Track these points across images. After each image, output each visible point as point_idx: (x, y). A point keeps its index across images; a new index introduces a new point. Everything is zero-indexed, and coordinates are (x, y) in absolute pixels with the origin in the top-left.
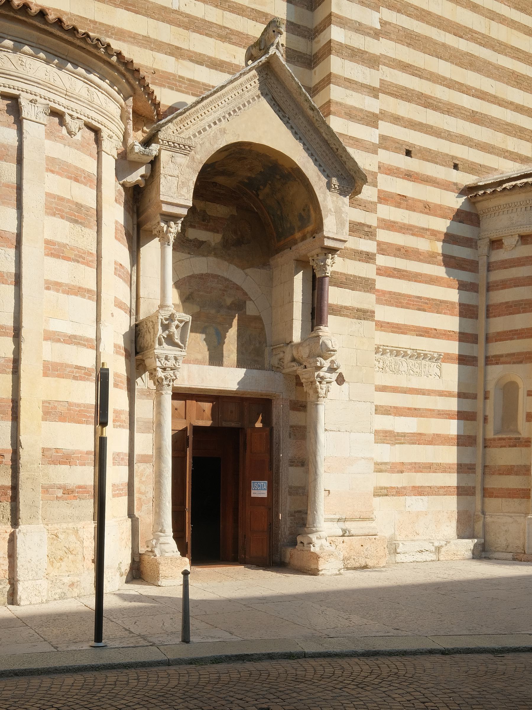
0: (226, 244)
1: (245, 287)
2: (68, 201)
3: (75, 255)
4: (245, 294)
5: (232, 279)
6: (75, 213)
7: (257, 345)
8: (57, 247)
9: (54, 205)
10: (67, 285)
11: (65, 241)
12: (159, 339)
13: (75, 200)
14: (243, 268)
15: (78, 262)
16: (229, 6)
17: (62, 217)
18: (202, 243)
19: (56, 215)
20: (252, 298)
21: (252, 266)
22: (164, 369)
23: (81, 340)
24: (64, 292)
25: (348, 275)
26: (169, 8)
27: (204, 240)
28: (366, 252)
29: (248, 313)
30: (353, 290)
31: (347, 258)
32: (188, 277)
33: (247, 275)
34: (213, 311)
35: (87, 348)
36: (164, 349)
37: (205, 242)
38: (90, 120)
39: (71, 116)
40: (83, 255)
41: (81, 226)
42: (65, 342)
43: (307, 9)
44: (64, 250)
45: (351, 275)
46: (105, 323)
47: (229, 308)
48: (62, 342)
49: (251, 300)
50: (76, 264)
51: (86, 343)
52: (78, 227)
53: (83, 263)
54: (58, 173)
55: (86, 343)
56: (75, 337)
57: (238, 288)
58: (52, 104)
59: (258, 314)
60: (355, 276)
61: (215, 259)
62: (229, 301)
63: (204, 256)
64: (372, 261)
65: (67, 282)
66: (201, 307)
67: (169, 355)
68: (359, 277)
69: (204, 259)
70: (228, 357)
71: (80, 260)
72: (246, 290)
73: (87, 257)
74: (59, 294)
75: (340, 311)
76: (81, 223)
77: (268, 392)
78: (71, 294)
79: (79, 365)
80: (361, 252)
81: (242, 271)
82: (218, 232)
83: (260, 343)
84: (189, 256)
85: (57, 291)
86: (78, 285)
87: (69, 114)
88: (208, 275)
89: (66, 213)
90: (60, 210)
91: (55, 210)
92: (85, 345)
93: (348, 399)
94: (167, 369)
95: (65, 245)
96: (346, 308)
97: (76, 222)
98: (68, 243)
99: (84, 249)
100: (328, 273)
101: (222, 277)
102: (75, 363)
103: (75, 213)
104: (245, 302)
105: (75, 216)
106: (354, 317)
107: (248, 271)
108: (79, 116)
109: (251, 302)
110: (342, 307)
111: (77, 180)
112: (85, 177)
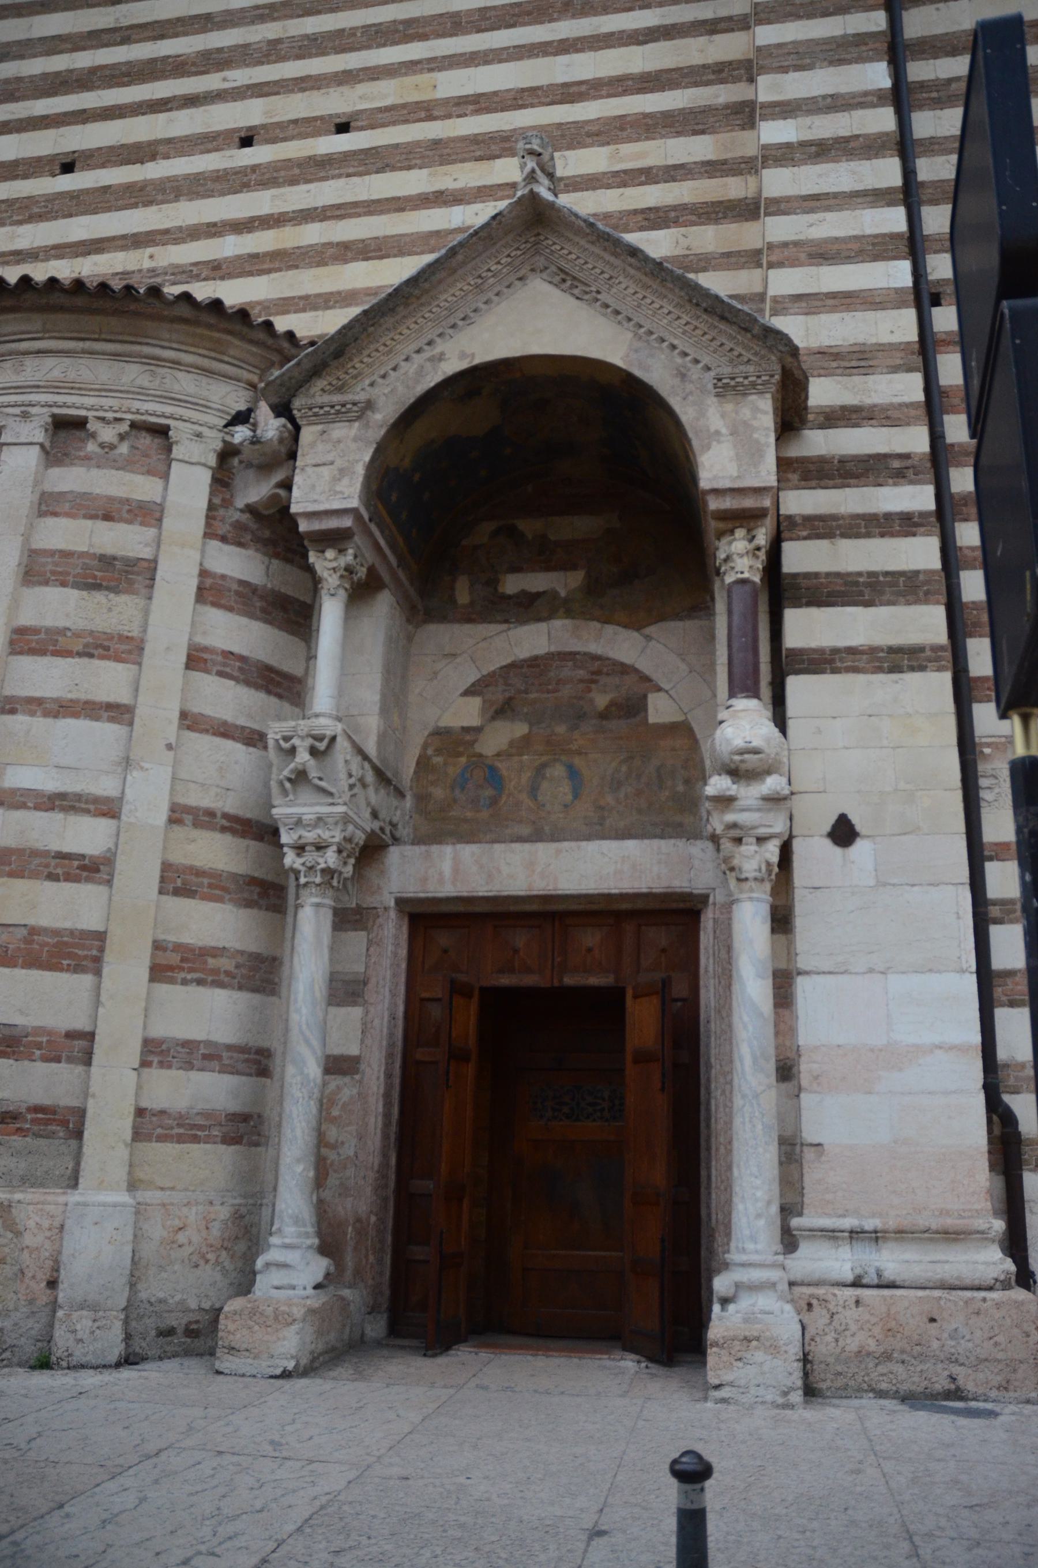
0: (593, 589)
1: (644, 665)
2: (82, 555)
3: (86, 646)
4: (647, 679)
5: (612, 654)
6: (96, 573)
7: (681, 788)
8: (43, 636)
9: (50, 567)
10: (55, 700)
11: (61, 623)
12: (281, 784)
13: (99, 551)
14: (637, 626)
15: (91, 656)
16: (566, 185)
17: (64, 584)
18: (539, 595)
19: (51, 583)
20: (662, 685)
21: (662, 618)
22: (300, 849)
23: (79, 801)
24: (47, 714)
25: (849, 574)
26: (445, 230)
27: (541, 590)
28: (901, 513)
29: (652, 719)
30: (868, 604)
31: (844, 536)
32: (502, 668)
33: (648, 638)
34: (561, 729)
35: (95, 816)
36: (291, 804)
37: (544, 592)
38: (139, 417)
39: (102, 419)
40: (106, 643)
41: (107, 593)
42: (37, 808)
43: (743, 129)
44: (60, 639)
45: (859, 574)
46: (142, 764)
47: (604, 715)
48: (29, 808)
49: (659, 689)
50: (85, 660)
51: (92, 807)
52: (99, 597)
53: (102, 657)
54: (68, 515)
55: (92, 807)
56: (62, 796)
57: (624, 669)
58: (57, 411)
59: (682, 718)
60: (871, 574)
61: (567, 622)
62: (602, 700)
63: (539, 620)
64: (922, 529)
65: (54, 694)
66: (531, 725)
67: (304, 817)
68: (887, 574)
69: (543, 626)
70: (601, 825)
71: (96, 652)
72: (647, 672)
73: (117, 646)
74: (35, 719)
75: (831, 661)
76: (108, 589)
77: (669, 890)
78: (64, 717)
79: (66, 849)
80: (888, 516)
81: (635, 634)
82: (574, 567)
83: (687, 782)
84: (505, 626)
85: (32, 714)
86: (83, 697)
87: (99, 418)
88: (551, 656)
89: (74, 577)
90: (60, 573)
91: (48, 575)
92: (88, 811)
93: (872, 883)
94: (307, 848)
95: (63, 631)
96: (852, 651)
97: (97, 587)
98: (68, 624)
99: (109, 631)
100: (742, 573)
101: (585, 654)
102: (55, 846)
103: (96, 573)
104: (645, 697)
105: (95, 577)
106: (879, 670)
107: (651, 630)
108: (118, 415)
109: (661, 694)
110: (835, 651)
111: (108, 517)
112: (129, 511)
